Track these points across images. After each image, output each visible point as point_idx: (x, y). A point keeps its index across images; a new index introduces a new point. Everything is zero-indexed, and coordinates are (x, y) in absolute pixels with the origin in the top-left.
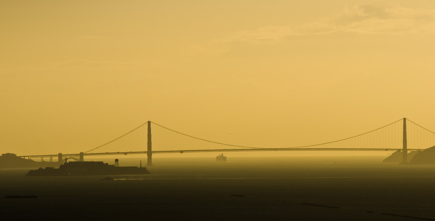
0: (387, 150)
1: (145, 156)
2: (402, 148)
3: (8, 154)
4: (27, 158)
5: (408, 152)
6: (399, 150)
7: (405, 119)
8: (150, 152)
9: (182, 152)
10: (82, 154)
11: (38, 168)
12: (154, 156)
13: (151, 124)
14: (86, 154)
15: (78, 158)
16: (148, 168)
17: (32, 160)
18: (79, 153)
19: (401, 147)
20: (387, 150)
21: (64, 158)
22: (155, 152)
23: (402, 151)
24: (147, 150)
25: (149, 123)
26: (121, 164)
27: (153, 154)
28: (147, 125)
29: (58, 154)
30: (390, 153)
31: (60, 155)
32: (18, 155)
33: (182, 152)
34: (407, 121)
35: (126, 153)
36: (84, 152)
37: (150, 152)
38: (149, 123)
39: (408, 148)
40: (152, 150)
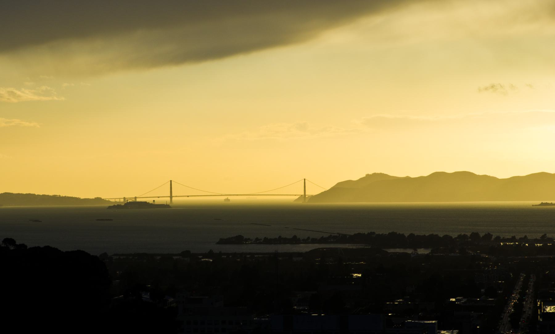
0: (295, 195)
1: (169, 199)
2: (303, 194)
3: (98, 198)
4: (107, 200)
5: (307, 196)
6: (302, 195)
7: (305, 179)
8: (171, 197)
9: (188, 196)
10: (136, 198)
11: (113, 205)
12: (173, 199)
13: (172, 182)
14: (138, 198)
15: (134, 199)
16: (170, 205)
17: (110, 201)
18: (134, 197)
19: (303, 194)
20: (295, 195)
21: (127, 199)
22: (174, 196)
23: (303, 196)
24: (169, 195)
25: (171, 181)
26: (156, 203)
27: (173, 198)
28: (170, 182)
29: (123, 197)
30: (297, 197)
31: (124, 198)
32: (102, 198)
33: (188, 196)
34: (306, 180)
35: (159, 197)
36: (137, 196)
37: (171, 197)
38: (171, 181)
39: (306, 194)
40: (173, 195)
